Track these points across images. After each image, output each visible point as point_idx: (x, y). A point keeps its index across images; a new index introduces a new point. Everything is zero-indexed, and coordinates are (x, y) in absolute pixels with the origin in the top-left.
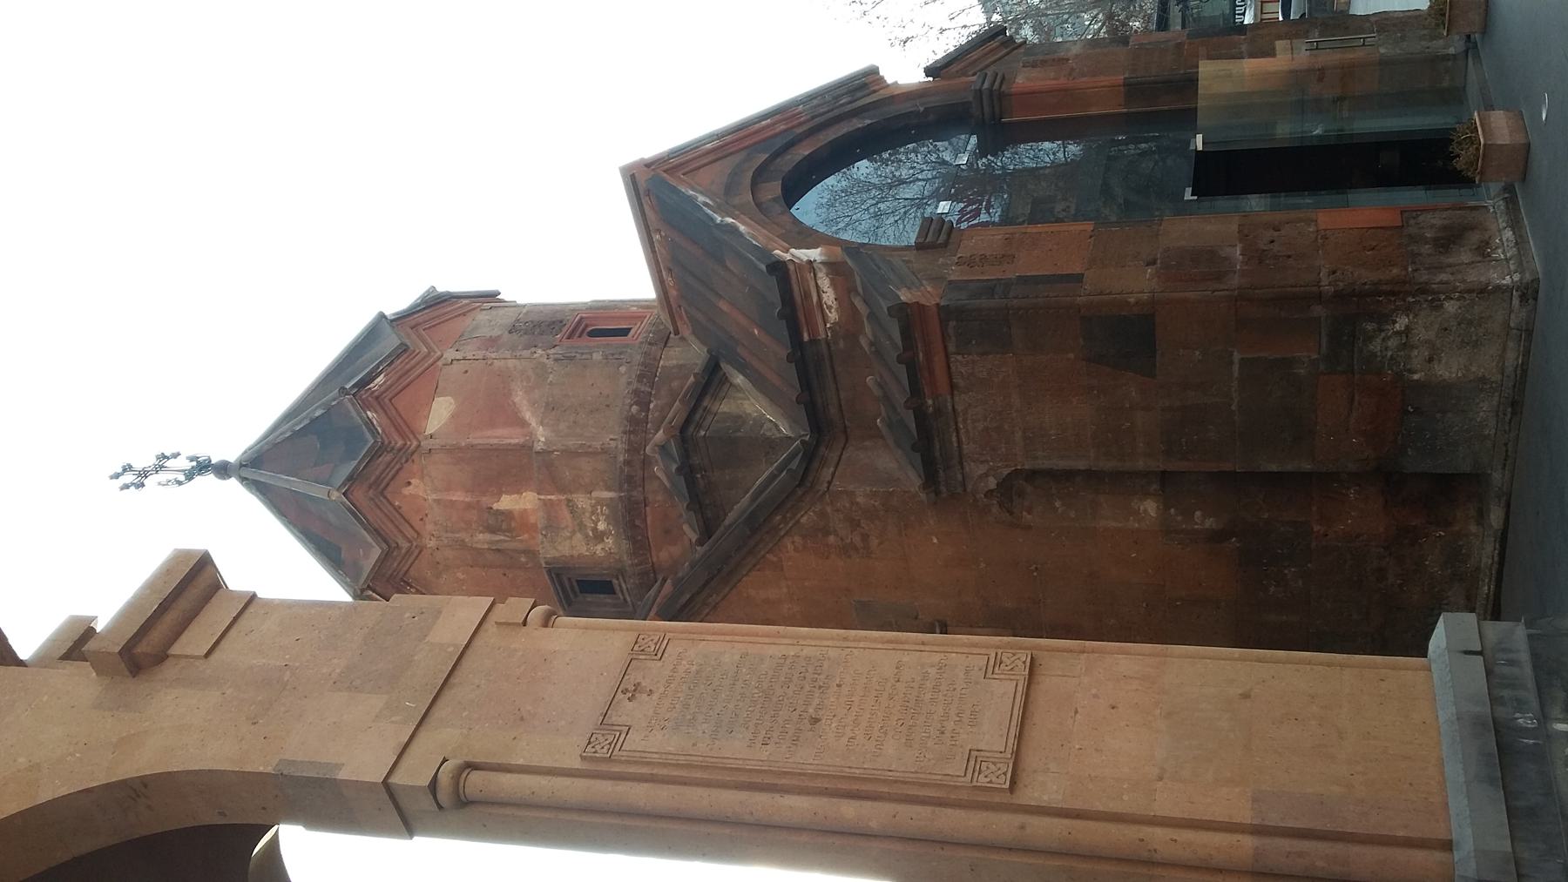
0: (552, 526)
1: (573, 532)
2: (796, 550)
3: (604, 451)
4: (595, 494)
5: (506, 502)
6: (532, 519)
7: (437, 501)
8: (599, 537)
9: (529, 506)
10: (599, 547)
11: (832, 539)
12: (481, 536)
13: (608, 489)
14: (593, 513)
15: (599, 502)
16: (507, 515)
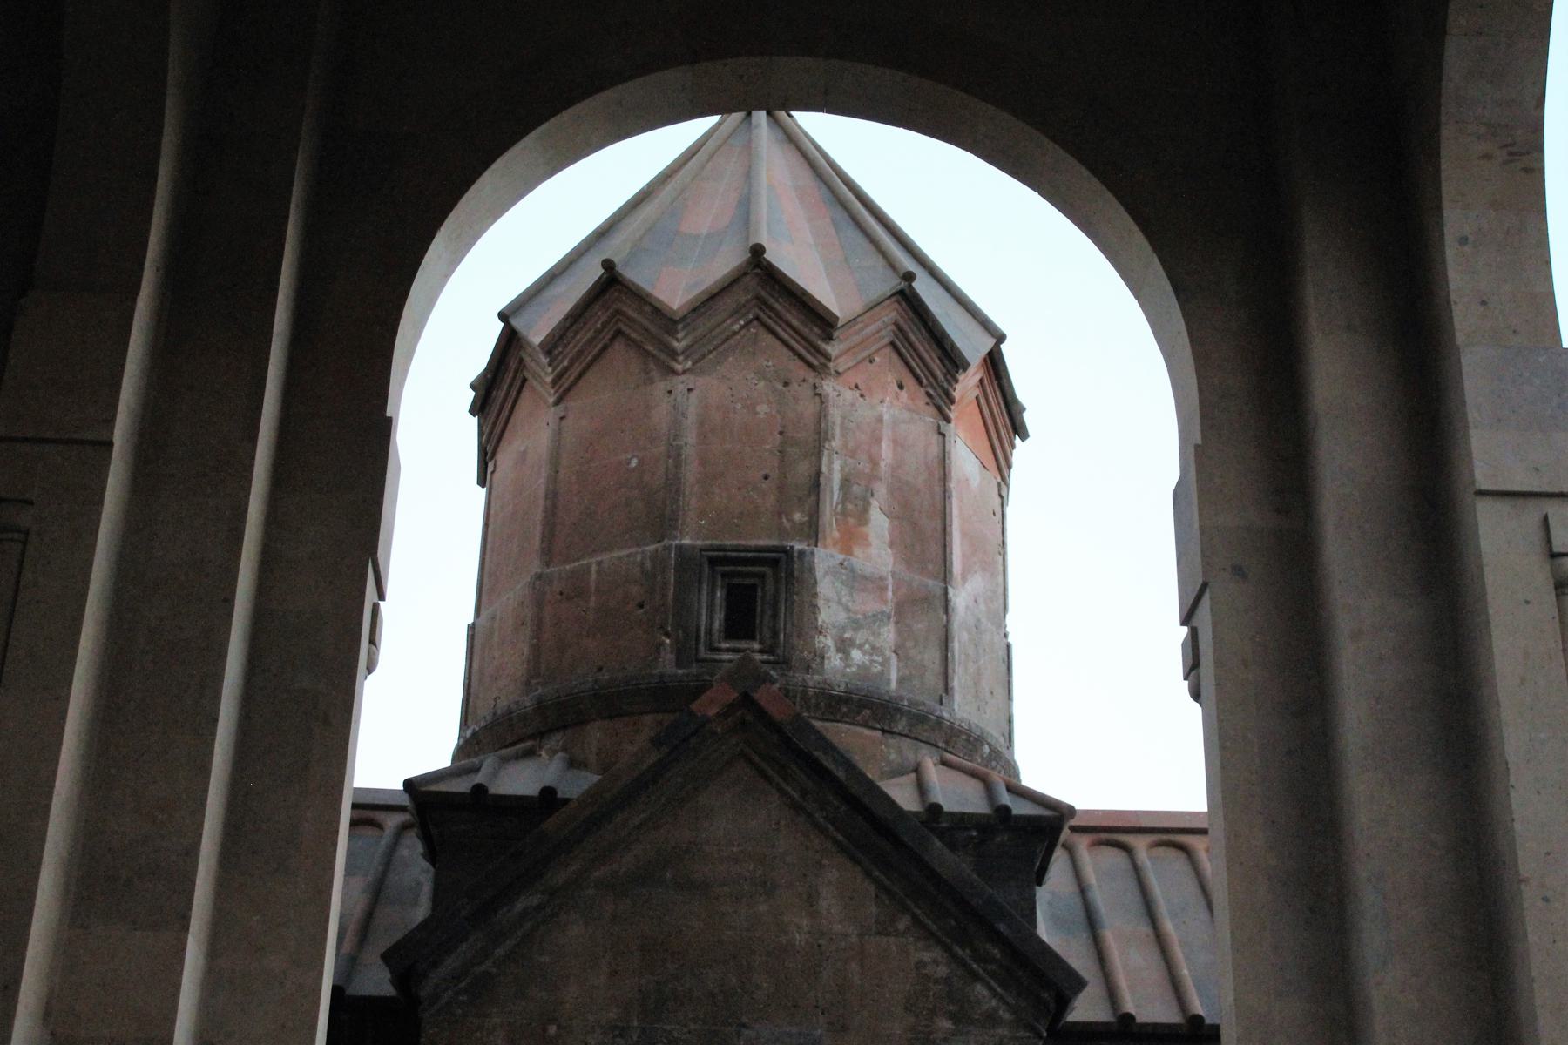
0: (857, 580)
1: (848, 610)
2: (920, 964)
3: (947, 689)
4: (894, 660)
5: (879, 523)
6: (857, 551)
7: (880, 420)
8: (844, 647)
9: (873, 551)
10: (830, 642)
11: (947, 1024)
12: (837, 466)
13: (901, 681)
14: (873, 648)
15: (885, 663)
16: (863, 516)
